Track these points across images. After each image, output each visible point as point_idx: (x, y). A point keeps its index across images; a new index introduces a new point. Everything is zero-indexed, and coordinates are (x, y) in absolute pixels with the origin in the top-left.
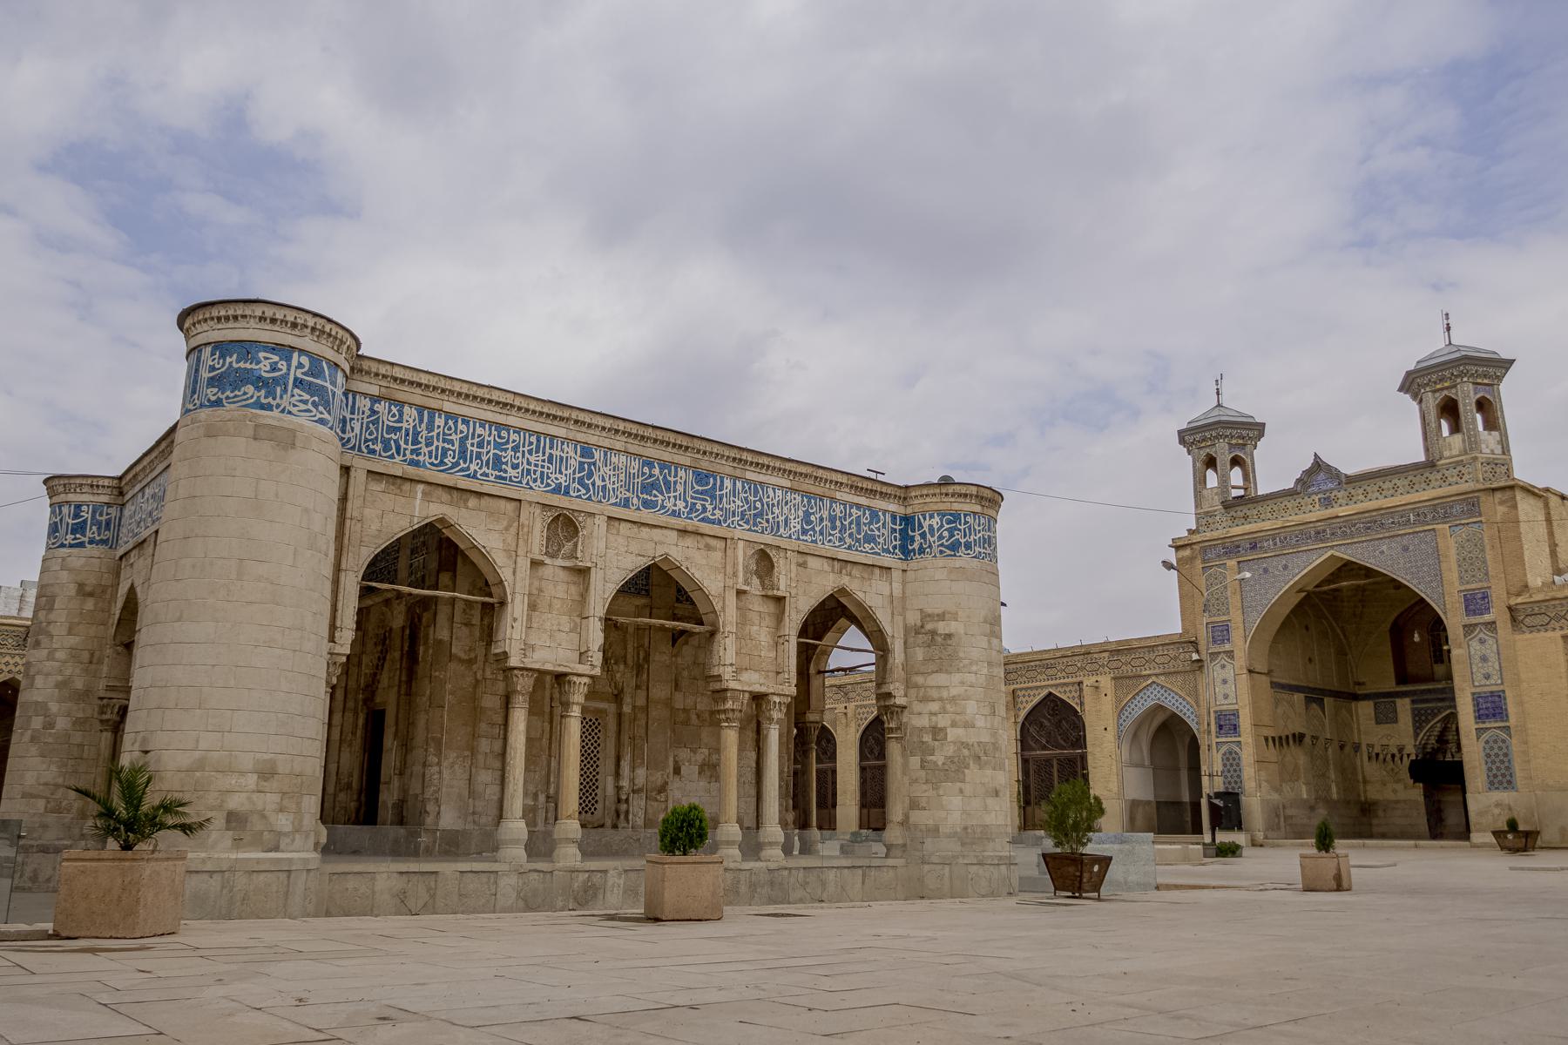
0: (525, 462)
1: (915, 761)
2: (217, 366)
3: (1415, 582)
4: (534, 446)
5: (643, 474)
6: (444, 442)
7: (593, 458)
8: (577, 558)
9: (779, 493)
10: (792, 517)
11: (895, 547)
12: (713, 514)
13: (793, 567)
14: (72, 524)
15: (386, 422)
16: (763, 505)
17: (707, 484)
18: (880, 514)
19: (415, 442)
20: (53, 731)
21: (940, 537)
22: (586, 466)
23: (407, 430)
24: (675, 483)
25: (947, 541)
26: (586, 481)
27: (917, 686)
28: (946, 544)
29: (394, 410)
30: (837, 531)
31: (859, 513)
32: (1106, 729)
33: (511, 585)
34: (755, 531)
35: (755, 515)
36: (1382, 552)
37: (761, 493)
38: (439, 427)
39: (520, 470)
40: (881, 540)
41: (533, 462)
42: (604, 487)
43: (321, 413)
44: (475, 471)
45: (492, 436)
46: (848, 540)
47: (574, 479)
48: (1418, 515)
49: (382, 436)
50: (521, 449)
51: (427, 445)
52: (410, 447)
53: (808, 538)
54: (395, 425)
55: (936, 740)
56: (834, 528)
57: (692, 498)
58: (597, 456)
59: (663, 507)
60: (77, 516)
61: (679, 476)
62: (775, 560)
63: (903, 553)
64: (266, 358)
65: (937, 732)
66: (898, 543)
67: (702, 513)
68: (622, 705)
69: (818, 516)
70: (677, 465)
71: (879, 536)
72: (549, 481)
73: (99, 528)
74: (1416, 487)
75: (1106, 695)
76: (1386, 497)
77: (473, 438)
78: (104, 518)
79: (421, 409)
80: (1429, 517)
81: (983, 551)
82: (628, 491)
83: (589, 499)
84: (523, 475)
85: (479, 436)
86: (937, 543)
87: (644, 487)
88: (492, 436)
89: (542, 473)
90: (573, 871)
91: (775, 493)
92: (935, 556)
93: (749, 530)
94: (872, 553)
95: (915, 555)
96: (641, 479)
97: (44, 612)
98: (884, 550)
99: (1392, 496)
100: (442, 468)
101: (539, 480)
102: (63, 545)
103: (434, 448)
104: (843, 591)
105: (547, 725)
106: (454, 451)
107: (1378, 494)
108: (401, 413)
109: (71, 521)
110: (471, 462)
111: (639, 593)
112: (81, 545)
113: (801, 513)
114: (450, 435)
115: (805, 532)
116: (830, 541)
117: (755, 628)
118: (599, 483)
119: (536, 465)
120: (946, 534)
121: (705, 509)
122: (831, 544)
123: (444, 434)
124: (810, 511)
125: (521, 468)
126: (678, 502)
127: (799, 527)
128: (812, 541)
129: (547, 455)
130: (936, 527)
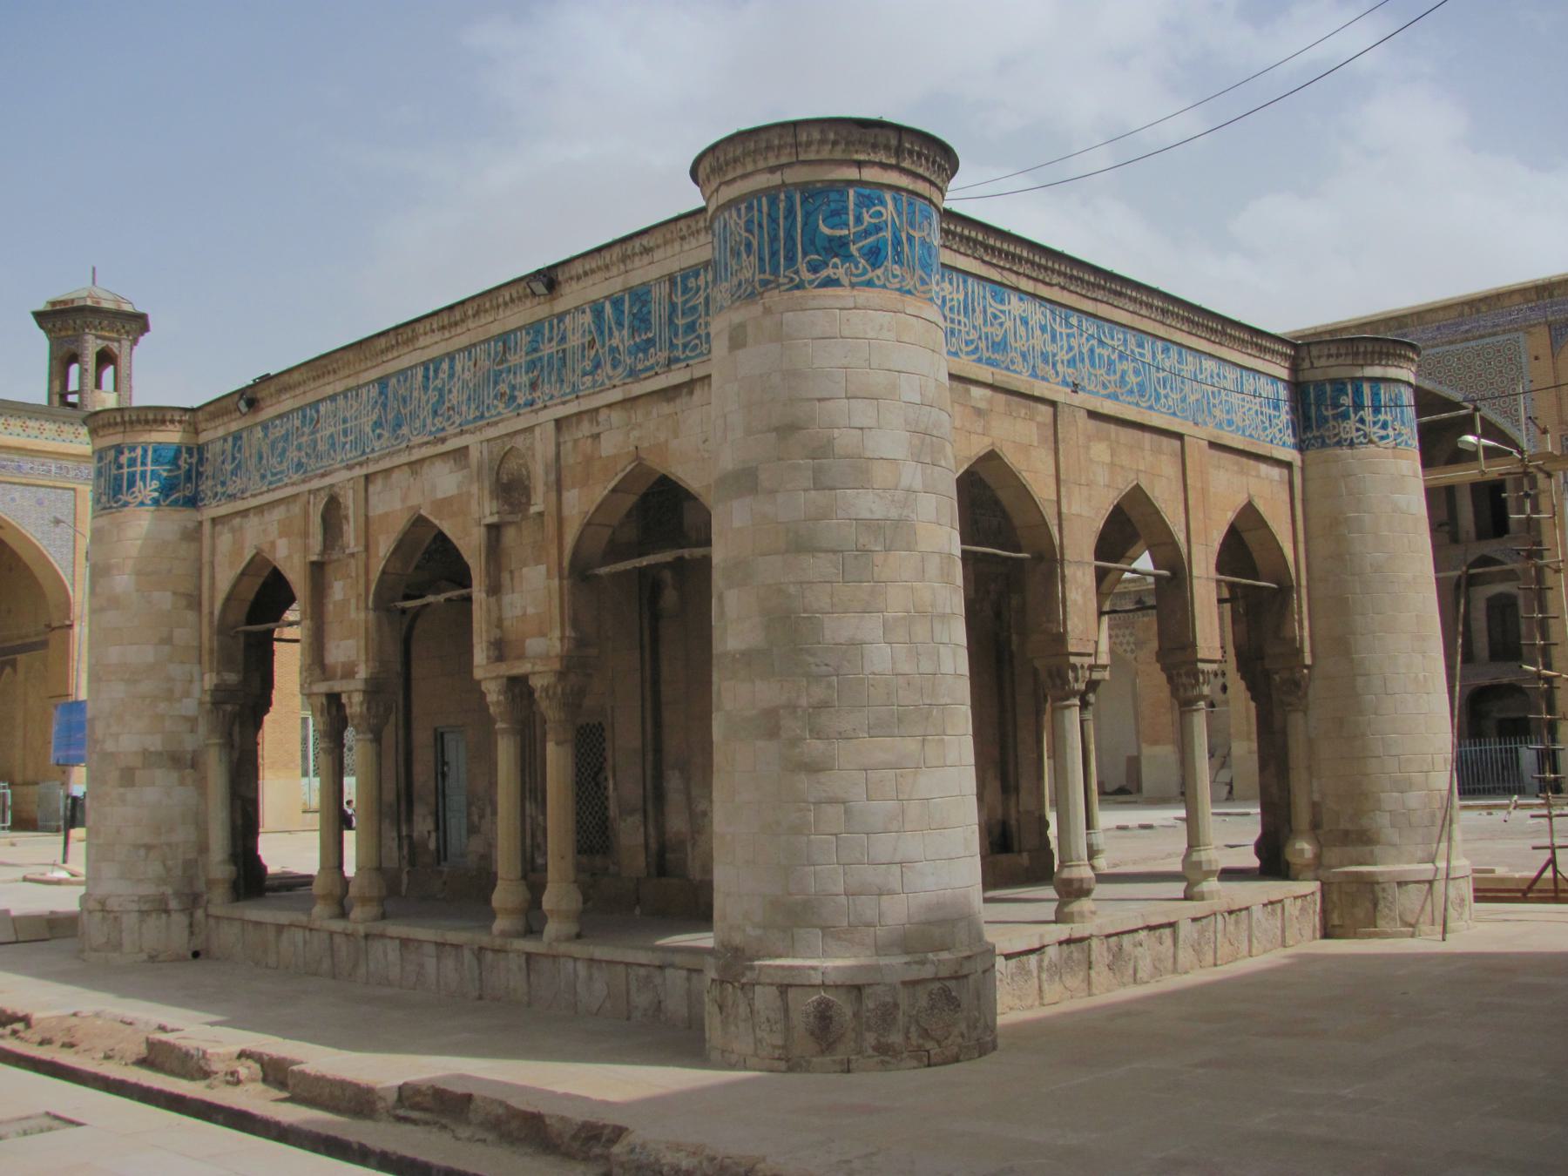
3: (45, 542)
36: (13, 500)
48: (61, 468)
74: (64, 436)
76: (29, 436)
80: (72, 474)
99: (36, 437)
107: (38, 432)
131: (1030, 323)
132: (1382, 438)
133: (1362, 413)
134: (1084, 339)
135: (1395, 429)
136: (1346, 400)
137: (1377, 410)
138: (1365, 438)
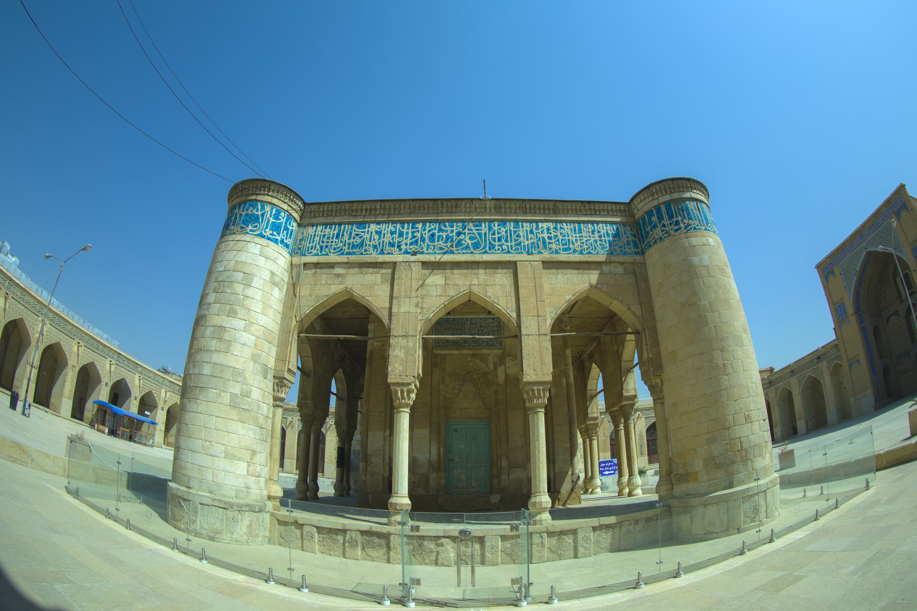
14: (272, 221)
20: (249, 400)
60: (277, 218)
73: (287, 234)
97: (242, 286)
112: (276, 241)
131: (383, 232)
132: (677, 230)
133: (663, 221)
134: (426, 231)
135: (684, 224)
136: (655, 219)
137: (671, 217)
138: (667, 234)
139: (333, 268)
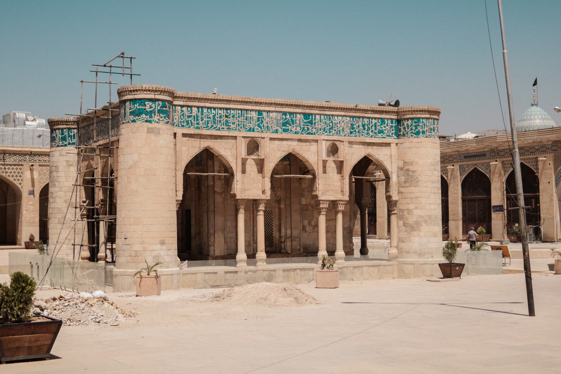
0: (237, 121)
1: (401, 223)
2: (132, 108)
4: (240, 114)
5: (283, 118)
6: (207, 118)
7: (263, 115)
8: (259, 155)
9: (340, 118)
10: (346, 127)
11: (392, 134)
12: (312, 131)
13: (347, 148)
15: (187, 114)
16: (333, 124)
17: (309, 119)
18: (386, 120)
19: (198, 120)
21: (411, 129)
22: (260, 119)
23: (194, 116)
24: (296, 120)
25: (415, 131)
26: (261, 125)
27: (402, 193)
28: (414, 132)
29: (189, 109)
30: (366, 130)
31: (376, 121)
32: (549, 183)
33: (235, 168)
34: (330, 135)
35: (330, 129)
37: (332, 118)
38: (205, 113)
39: (235, 125)
40: (386, 132)
41: (240, 120)
42: (268, 127)
43: (167, 120)
44: (219, 128)
45: (224, 113)
46: (371, 133)
47: (256, 125)
49: (186, 120)
50: (235, 116)
51: (202, 121)
52: (196, 122)
53: (353, 135)
54: (190, 115)
55: (409, 214)
56: (364, 129)
57: (303, 125)
58: (264, 114)
59: (291, 131)
60: (62, 134)
61: (297, 117)
62: (338, 146)
63: (396, 136)
64: (148, 104)
65: (409, 211)
66: (394, 131)
67: (307, 131)
68: (280, 204)
69: (357, 125)
70: (296, 113)
71: (385, 130)
72: (247, 127)
73: (71, 138)
75: (550, 164)
77: (217, 115)
78: (72, 134)
79: (198, 107)
81: (430, 134)
82: (277, 126)
83: (262, 132)
84: (237, 126)
85: (220, 114)
86: (410, 132)
87: (283, 124)
88: (224, 113)
89: (244, 124)
90: (264, 271)
91: (338, 118)
92: (409, 137)
93: (327, 135)
94: (382, 138)
95: (401, 137)
96: (282, 121)
97: (55, 173)
98: (387, 136)
100: (208, 128)
101: (243, 127)
102: (58, 146)
103: (204, 121)
104: (369, 155)
105: (252, 216)
106: (211, 121)
108: (191, 110)
109: (60, 136)
110: (217, 124)
111: (285, 159)
112: (66, 145)
113: (350, 125)
114: (209, 115)
115: (351, 133)
116: (363, 135)
117: (331, 174)
118: (266, 125)
119: (241, 122)
120: (414, 128)
121: (308, 129)
122: (363, 136)
123: (207, 115)
124: (354, 123)
125: (236, 124)
126: (297, 128)
127: (349, 131)
128: (355, 136)
129: (245, 117)
130: (410, 125)
139: (86, 151)
